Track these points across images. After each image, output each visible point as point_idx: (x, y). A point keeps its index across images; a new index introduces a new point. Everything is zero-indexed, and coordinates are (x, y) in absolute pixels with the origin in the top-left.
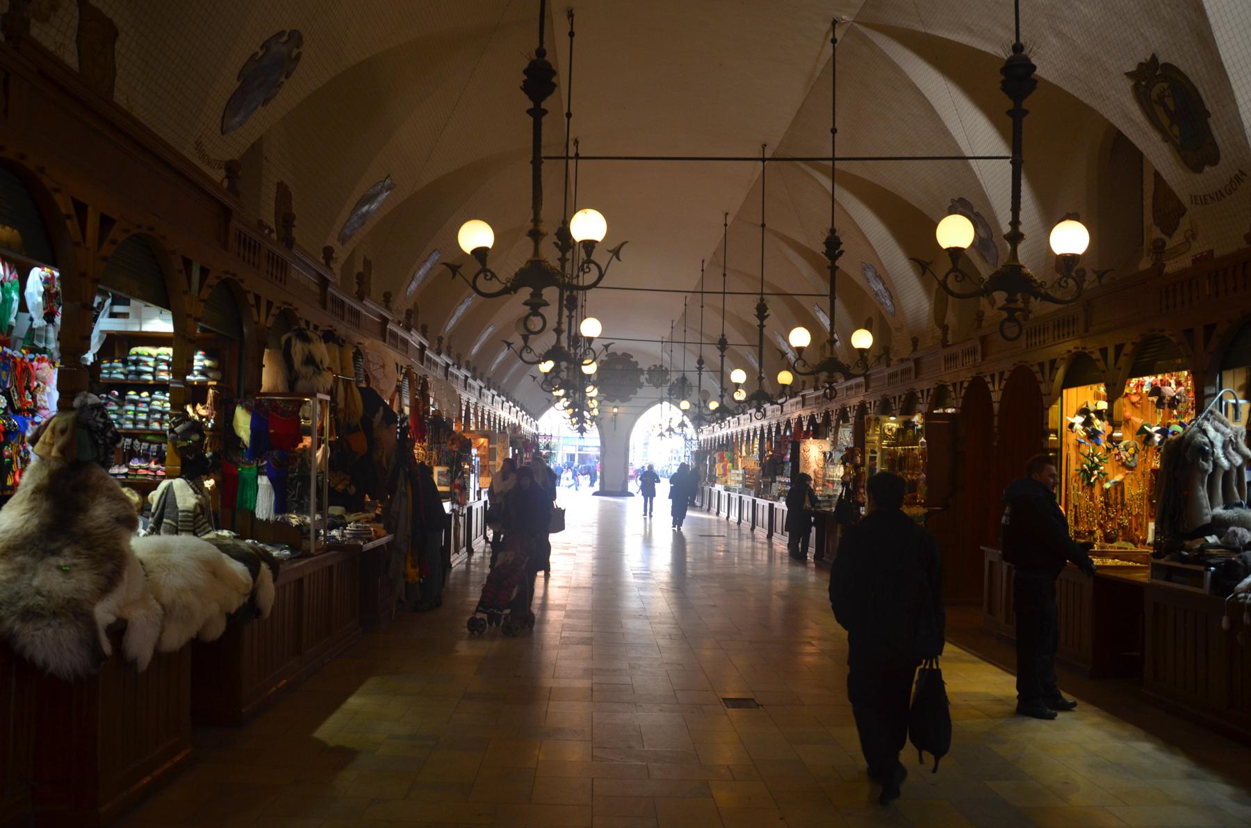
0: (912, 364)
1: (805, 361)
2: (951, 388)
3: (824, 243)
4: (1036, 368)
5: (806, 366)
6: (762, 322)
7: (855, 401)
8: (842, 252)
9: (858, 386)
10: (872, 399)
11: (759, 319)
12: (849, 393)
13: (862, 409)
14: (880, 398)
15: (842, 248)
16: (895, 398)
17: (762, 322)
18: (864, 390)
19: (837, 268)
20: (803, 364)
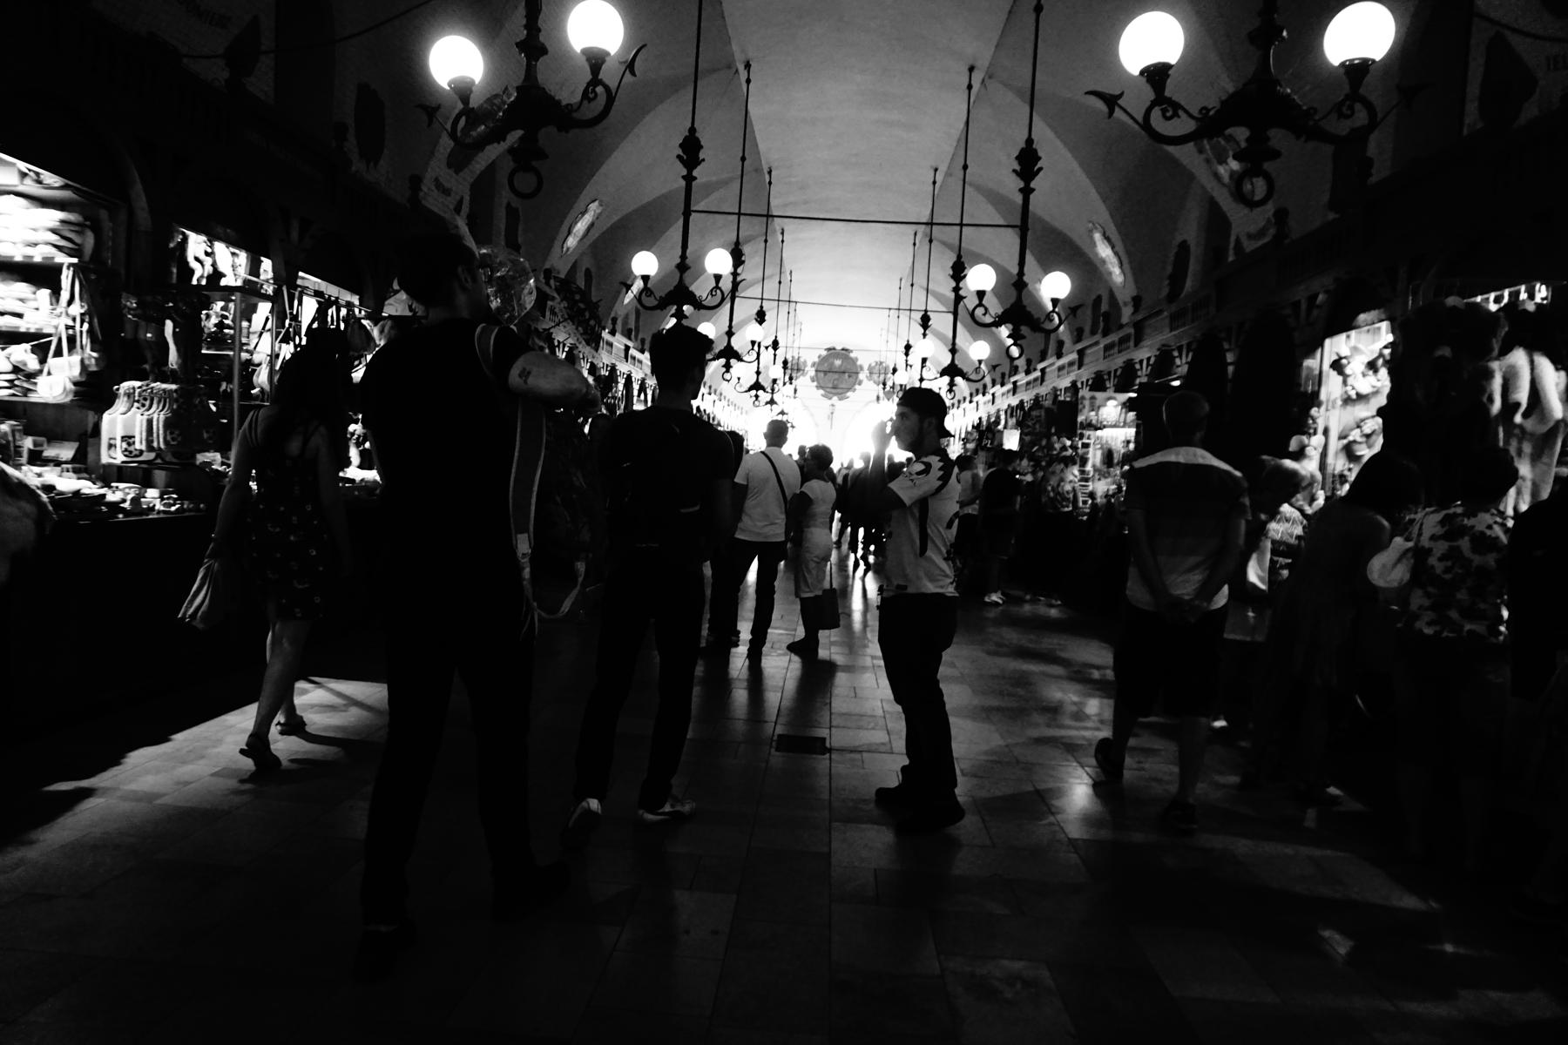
0: (1132, 331)
1: (986, 309)
2: (1176, 354)
3: (1017, 158)
4: (1288, 311)
5: (987, 315)
6: (958, 284)
7: (1065, 383)
8: (1040, 169)
9: (1071, 364)
10: (1085, 374)
11: (955, 280)
12: (1060, 373)
13: (1074, 388)
14: (1093, 376)
15: (1039, 165)
16: (1109, 373)
17: (958, 284)
18: (1076, 367)
19: (1033, 190)
20: (984, 312)
